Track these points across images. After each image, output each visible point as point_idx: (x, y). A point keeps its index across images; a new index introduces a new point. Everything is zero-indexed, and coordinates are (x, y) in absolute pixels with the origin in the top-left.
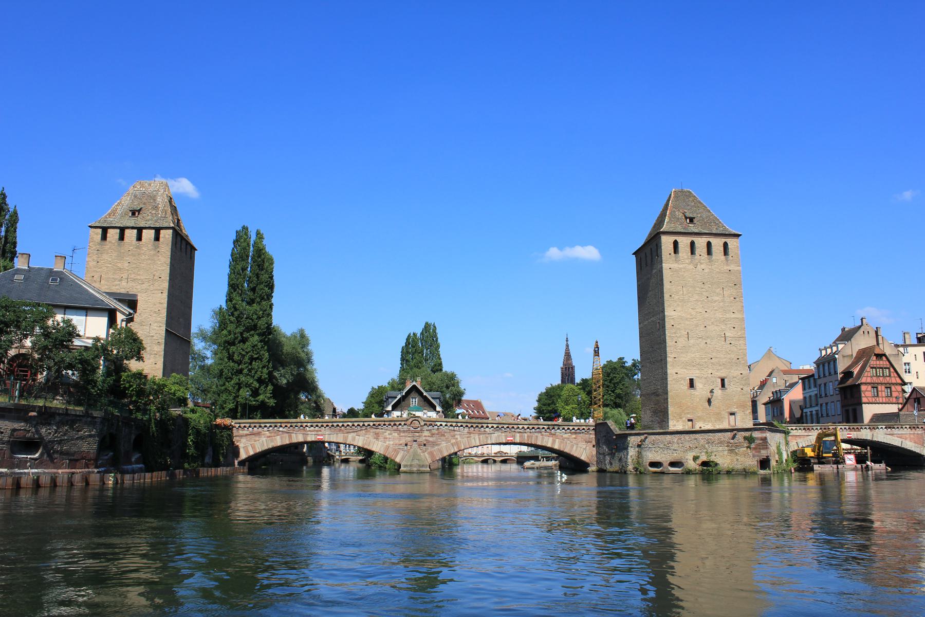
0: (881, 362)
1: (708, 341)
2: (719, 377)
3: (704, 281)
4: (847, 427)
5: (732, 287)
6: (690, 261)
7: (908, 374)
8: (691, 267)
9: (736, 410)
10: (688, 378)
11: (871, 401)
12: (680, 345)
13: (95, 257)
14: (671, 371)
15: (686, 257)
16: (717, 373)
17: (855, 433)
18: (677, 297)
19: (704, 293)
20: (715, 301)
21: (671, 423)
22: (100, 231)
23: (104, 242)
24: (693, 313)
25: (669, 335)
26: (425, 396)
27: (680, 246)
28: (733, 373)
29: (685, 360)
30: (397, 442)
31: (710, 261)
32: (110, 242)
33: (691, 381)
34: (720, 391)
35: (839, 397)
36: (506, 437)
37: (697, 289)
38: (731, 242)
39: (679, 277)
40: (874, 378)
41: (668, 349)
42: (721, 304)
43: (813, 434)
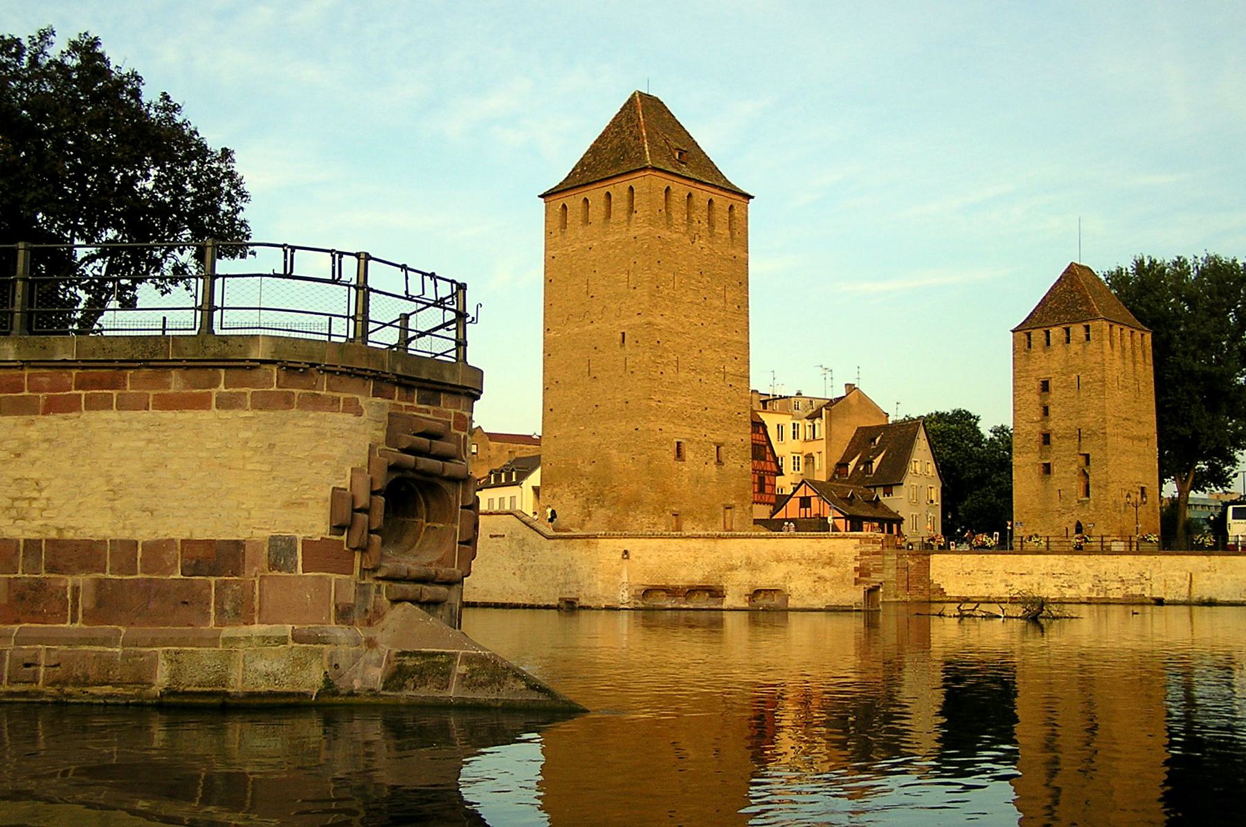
1: (703, 378)
2: (715, 443)
3: (703, 269)
5: (735, 286)
6: (686, 228)
9: (734, 502)
10: (675, 440)
15: (680, 221)
16: (712, 436)
18: (666, 292)
20: (715, 308)
28: (732, 437)
29: (672, 408)
37: (693, 281)
42: (723, 314)
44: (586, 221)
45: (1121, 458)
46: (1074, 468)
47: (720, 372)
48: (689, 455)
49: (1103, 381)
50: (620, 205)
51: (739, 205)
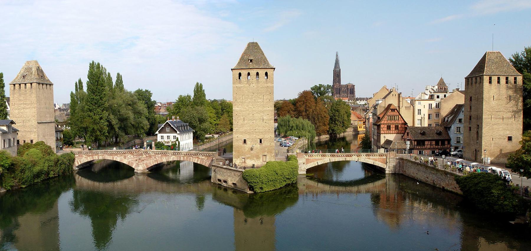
0: (394, 113)
1: (254, 122)
2: (259, 139)
3: (254, 92)
4: (345, 155)
5: (268, 94)
7: (419, 115)
10: (243, 139)
11: (386, 133)
15: (245, 81)
17: (349, 158)
18: (239, 101)
19: (253, 98)
20: (259, 102)
24: (247, 108)
25: (234, 119)
31: (258, 82)
34: (259, 145)
37: (250, 96)
38: (269, 71)
39: (240, 91)
40: (389, 121)
42: (262, 103)
43: (326, 158)
45: (493, 127)
46: (476, 130)
47: (262, 119)
48: (248, 142)
49: (483, 99)
51: (269, 71)
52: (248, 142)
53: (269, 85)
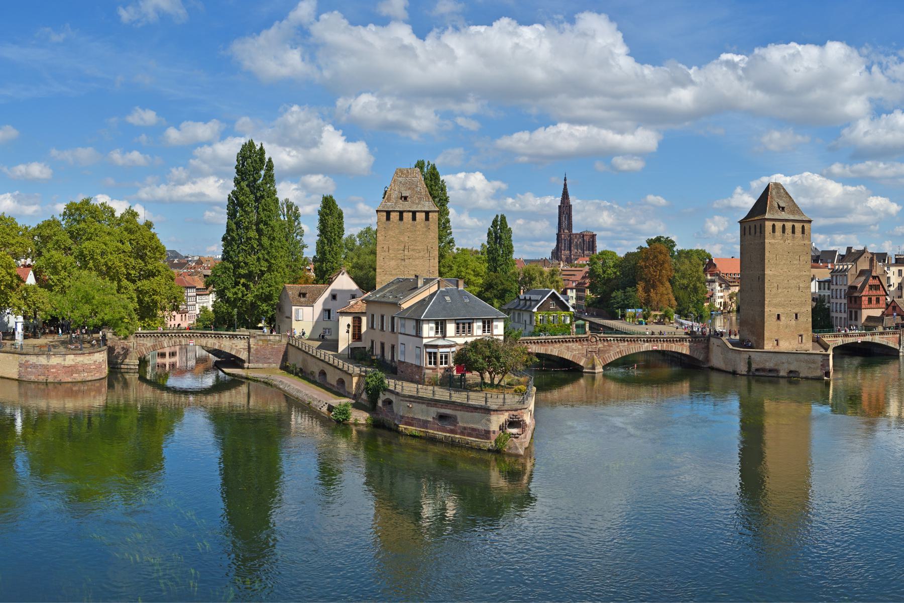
8: (782, 242)
12: (773, 293)
13: (383, 233)
14: (767, 309)
21: (766, 342)
22: (385, 214)
23: (388, 222)
24: (782, 272)
26: (562, 301)
27: (777, 227)
30: (581, 352)
32: (393, 222)
33: (779, 315)
35: (846, 301)
36: (653, 346)
41: (766, 296)
44: (750, 233)
50: (758, 230)
52: (782, 318)
53: (806, 242)
